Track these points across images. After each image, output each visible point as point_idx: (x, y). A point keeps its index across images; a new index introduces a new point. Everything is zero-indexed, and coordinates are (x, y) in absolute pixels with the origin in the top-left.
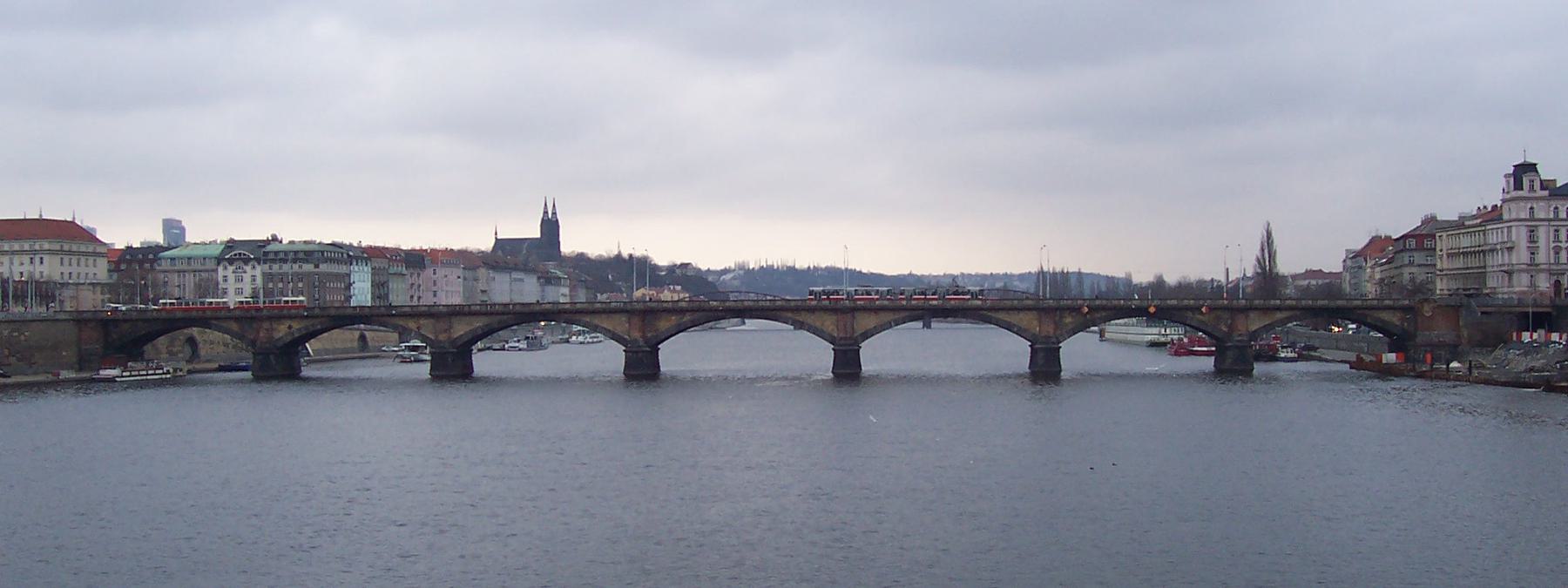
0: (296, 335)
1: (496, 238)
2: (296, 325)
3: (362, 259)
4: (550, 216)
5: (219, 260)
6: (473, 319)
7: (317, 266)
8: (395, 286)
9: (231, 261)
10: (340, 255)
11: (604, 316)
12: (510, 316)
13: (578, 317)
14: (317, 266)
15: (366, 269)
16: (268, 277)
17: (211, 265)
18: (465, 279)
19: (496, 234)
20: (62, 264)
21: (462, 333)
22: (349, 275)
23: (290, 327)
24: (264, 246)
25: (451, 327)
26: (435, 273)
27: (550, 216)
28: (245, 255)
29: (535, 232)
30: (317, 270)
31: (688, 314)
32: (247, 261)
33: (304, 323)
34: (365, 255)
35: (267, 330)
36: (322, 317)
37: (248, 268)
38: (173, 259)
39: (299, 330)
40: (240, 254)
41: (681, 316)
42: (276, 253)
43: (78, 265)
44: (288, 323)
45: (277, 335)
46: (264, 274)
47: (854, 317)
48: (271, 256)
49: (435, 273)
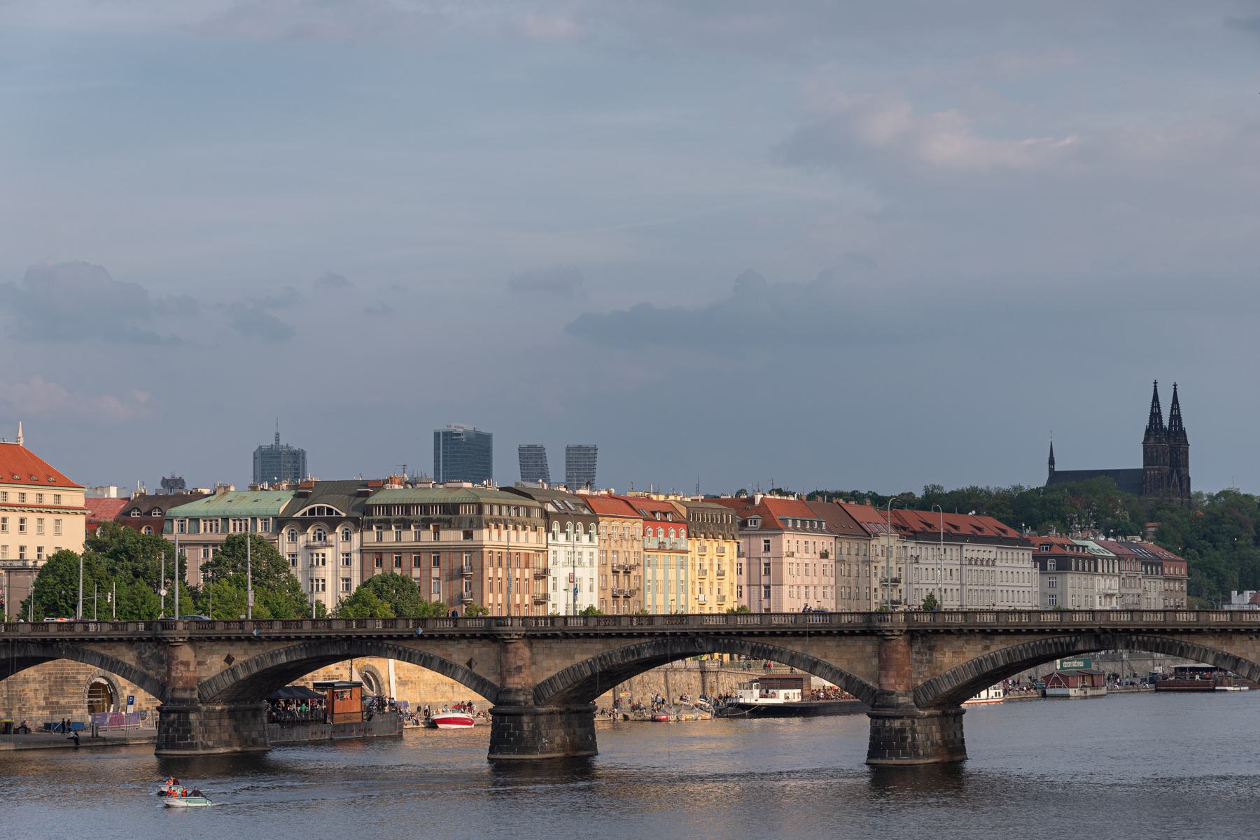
0: (242, 675)
1: (1051, 471)
2: (241, 655)
3: (577, 517)
4: (1166, 423)
5: (280, 522)
6: (573, 645)
7: (468, 535)
8: (660, 575)
9: (304, 524)
10: (523, 512)
11: (830, 643)
12: (643, 640)
13: (777, 643)
14: (468, 535)
18: (840, 561)
19: (1052, 461)
21: (552, 674)
22: (543, 552)
23: (229, 660)
24: (367, 494)
26: (767, 549)
27: (1166, 423)
28: (330, 511)
29: (1133, 459)
30: (468, 542)
31: (998, 639)
32: (333, 523)
33: (254, 652)
34: (586, 512)
36: (288, 639)
39: (246, 665)
40: (320, 510)
41: (988, 642)
42: (388, 508)
43: (40, 532)
44: (226, 650)
45: (206, 675)
46: (363, 551)
48: (379, 515)
49: (767, 549)
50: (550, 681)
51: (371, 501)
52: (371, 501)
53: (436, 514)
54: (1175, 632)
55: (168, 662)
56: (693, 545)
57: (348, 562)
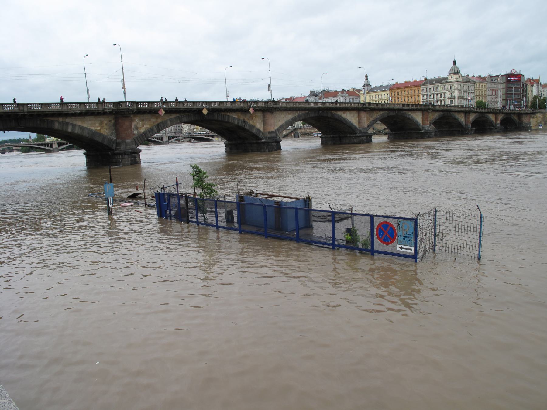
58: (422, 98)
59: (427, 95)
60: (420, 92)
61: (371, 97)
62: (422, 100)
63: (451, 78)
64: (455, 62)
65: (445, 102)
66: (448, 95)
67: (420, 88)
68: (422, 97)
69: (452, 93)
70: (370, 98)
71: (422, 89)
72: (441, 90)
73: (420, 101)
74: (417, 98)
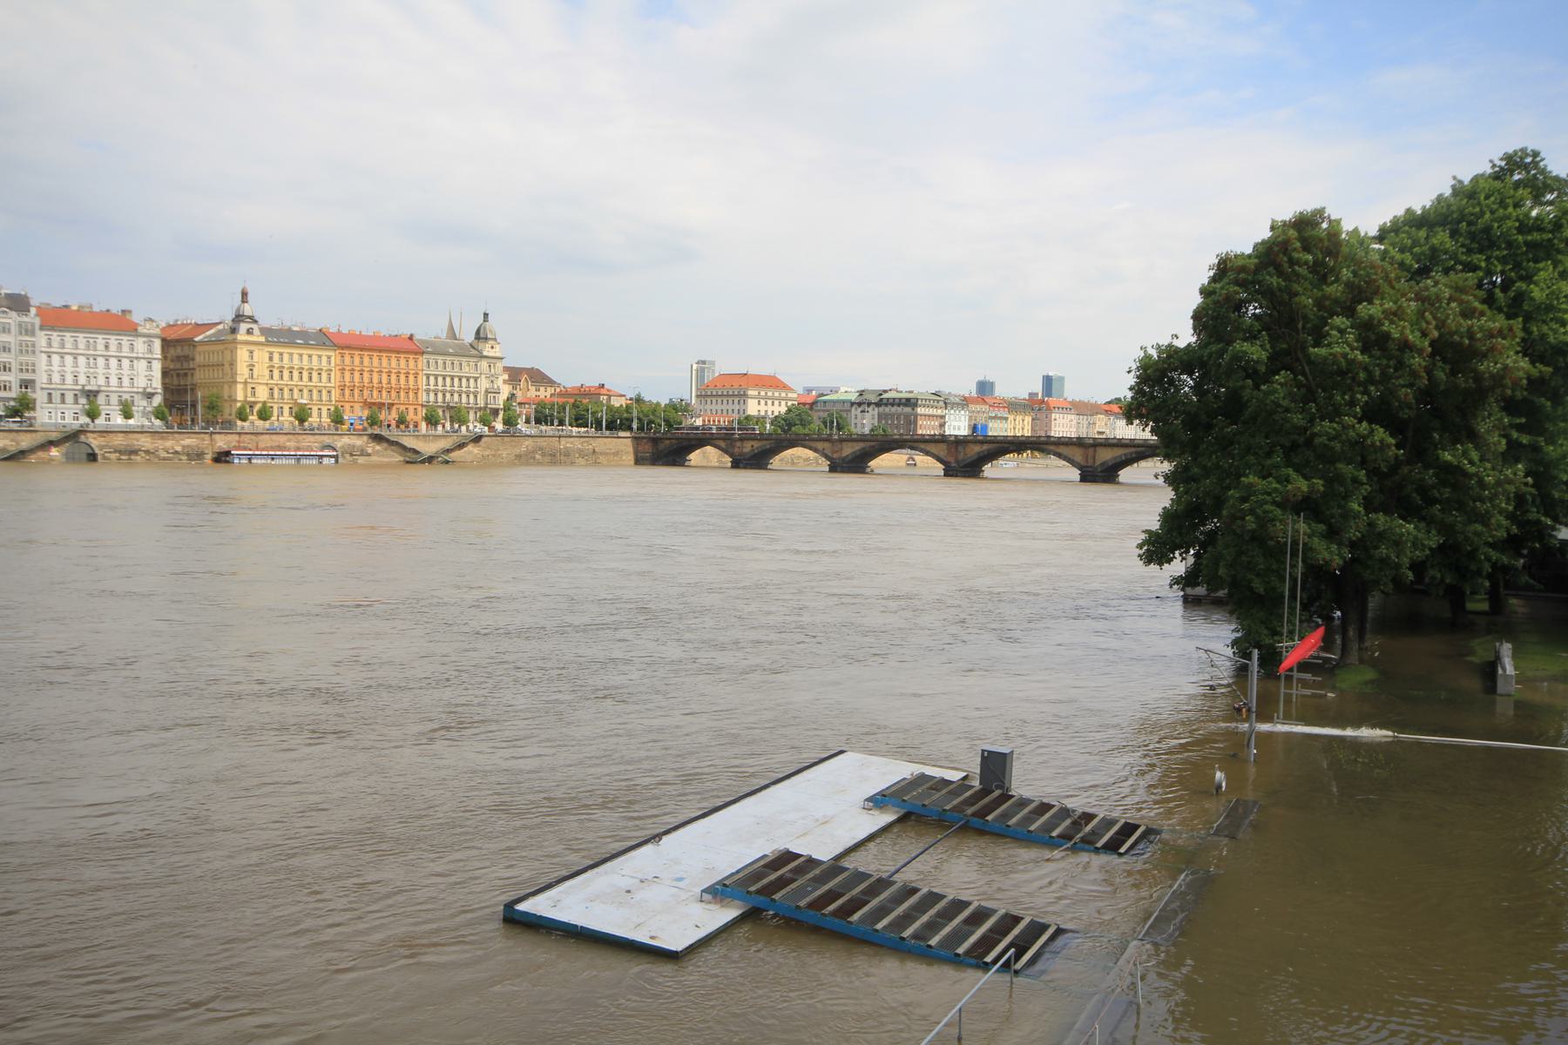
0: (756, 451)
6: (855, 444)
11: (933, 445)
13: (916, 445)
14: (913, 409)
15: (963, 412)
16: (879, 415)
17: (847, 406)
20: (759, 404)
23: (752, 446)
25: (842, 449)
32: (869, 404)
35: (739, 447)
37: (870, 409)
38: (825, 402)
39: (757, 448)
42: (888, 399)
47: (1095, 451)
48: (885, 401)
50: (848, 455)
51: (882, 397)
52: (882, 397)
53: (904, 401)
54: (1040, 444)
55: (733, 447)
56: (1011, 417)
57: (873, 419)
58: (424, 383)
59: (436, 377)
60: (420, 367)
61: (276, 357)
62: (425, 387)
63: (490, 349)
64: (486, 315)
65: (476, 397)
66: (484, 384)
67: (421, 359)
68: (425, 378)
69: (492, 382)
70: (271, 359)
71: (425, 361)
72: (467, 370)
73: (420, 387)
74: (411, 378)
